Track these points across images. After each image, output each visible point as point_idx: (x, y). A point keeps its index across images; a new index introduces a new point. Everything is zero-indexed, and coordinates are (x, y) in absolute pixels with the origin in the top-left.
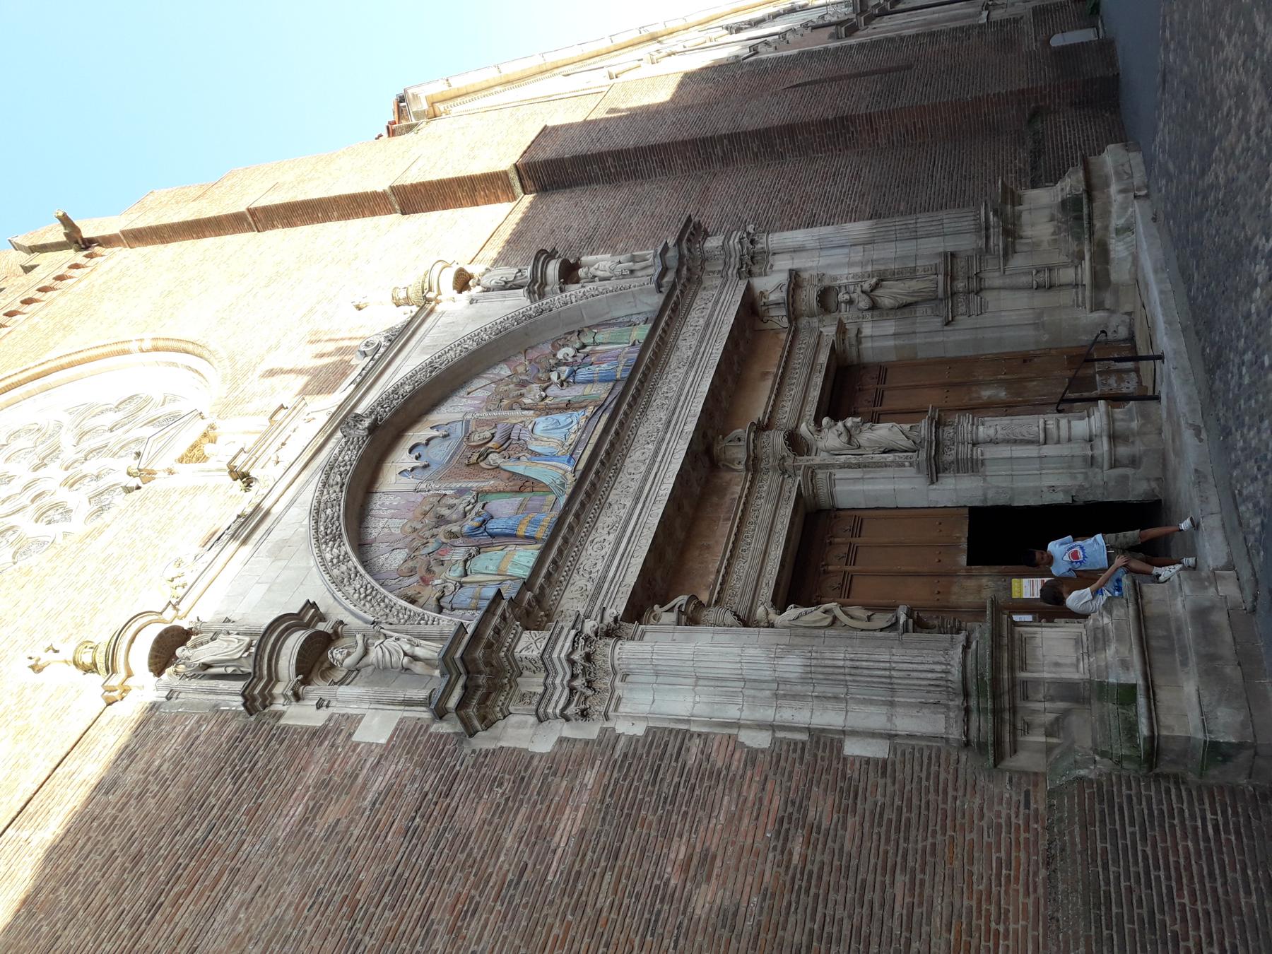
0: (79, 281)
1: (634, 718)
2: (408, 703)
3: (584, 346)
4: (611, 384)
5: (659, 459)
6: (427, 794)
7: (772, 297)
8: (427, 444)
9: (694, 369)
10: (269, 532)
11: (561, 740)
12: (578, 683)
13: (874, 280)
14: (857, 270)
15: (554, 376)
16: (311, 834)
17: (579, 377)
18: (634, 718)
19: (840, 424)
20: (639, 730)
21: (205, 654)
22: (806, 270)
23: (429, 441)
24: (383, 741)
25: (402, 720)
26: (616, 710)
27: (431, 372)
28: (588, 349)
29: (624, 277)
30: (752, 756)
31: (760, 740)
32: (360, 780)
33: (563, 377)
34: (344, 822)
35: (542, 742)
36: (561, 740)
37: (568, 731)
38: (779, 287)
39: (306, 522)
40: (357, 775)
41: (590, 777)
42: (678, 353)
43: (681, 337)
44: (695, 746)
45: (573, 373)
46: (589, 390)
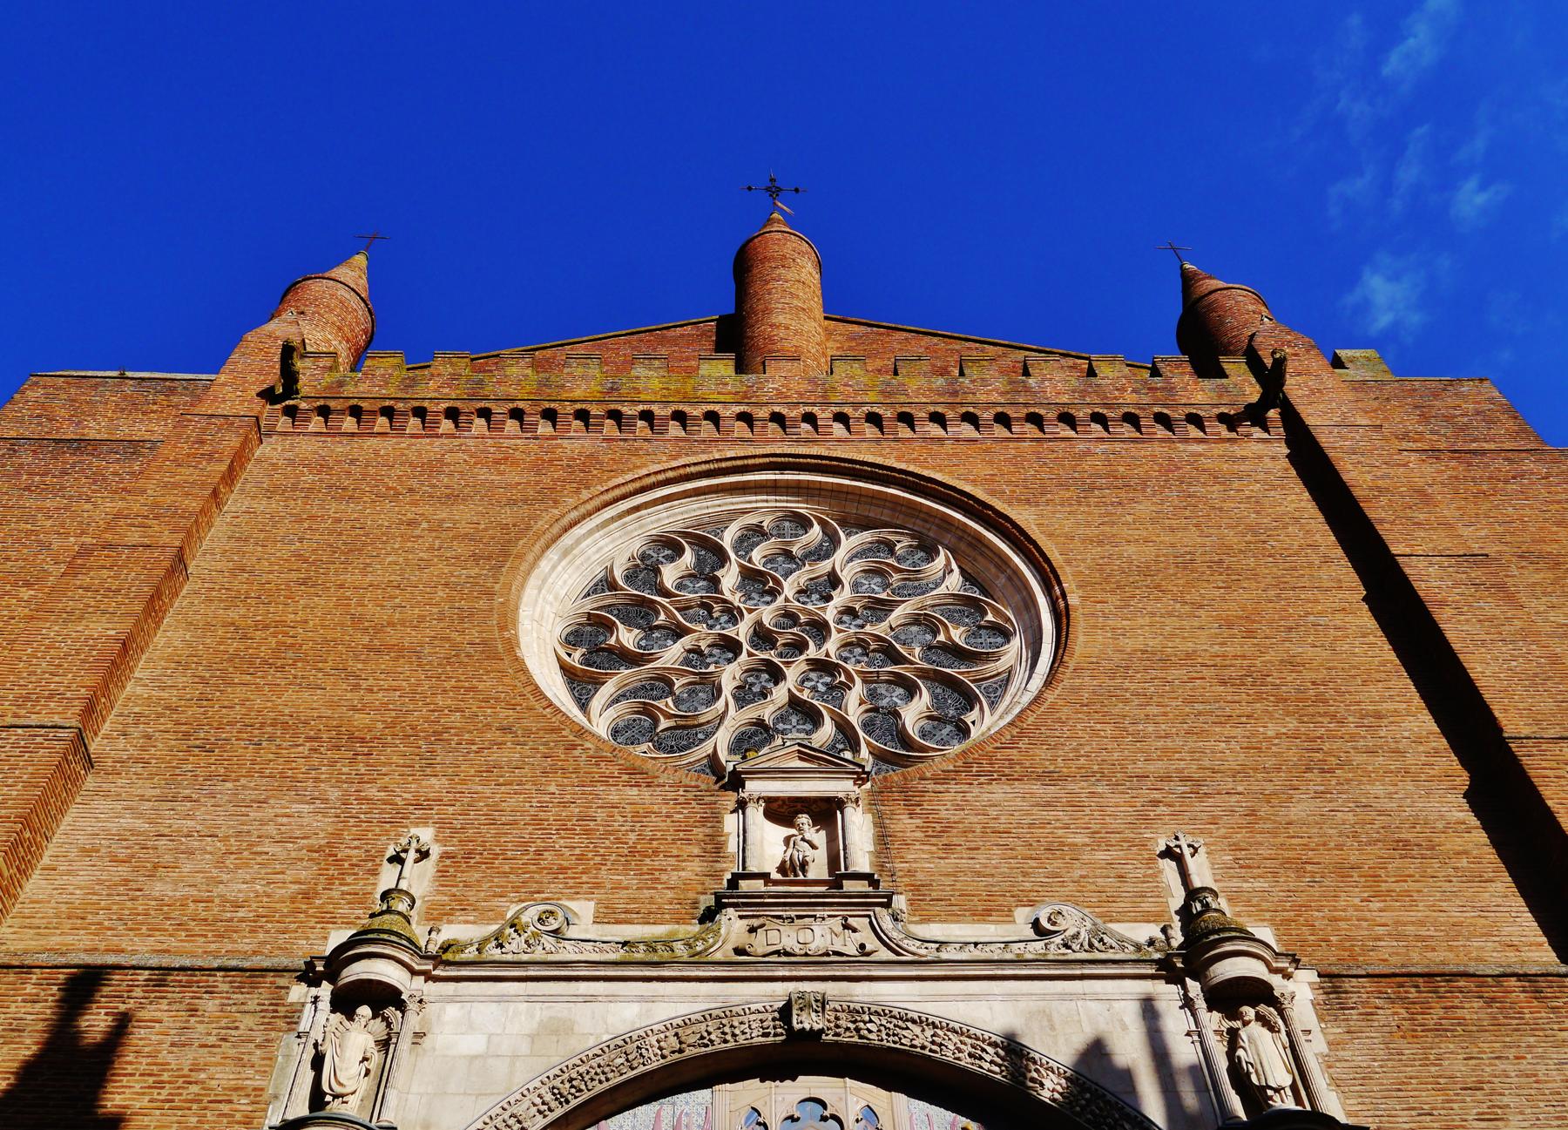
8: (824, 1119)
10: (590, 999)
23: (835, 1118)
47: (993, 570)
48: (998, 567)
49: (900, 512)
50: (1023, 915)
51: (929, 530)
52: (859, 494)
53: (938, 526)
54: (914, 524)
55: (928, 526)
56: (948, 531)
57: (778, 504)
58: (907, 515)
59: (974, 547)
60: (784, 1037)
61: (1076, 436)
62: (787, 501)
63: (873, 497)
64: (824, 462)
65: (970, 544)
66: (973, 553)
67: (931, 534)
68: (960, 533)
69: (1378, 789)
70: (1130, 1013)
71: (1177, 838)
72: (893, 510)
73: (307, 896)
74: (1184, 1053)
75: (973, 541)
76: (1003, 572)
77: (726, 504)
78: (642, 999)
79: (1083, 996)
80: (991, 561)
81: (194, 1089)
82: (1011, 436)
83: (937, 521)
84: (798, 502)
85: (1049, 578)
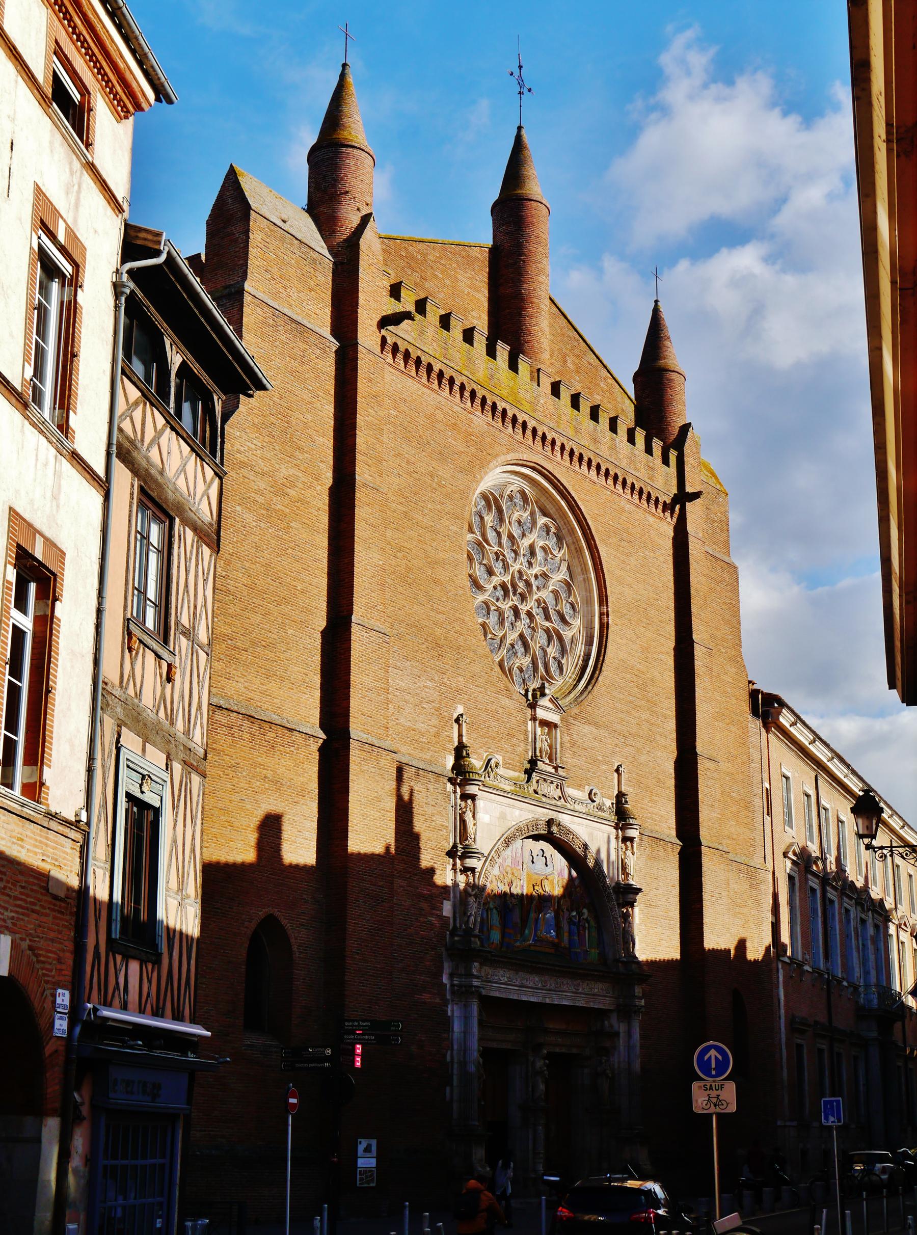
0: (654, 515)
1: (453, 1011)
2: (455, 920)
3: (588, 923)
4: (567, 946)
5: (536, 991)
6: (431, 940)
7: (606, 1022)
9: (573, 995)
10: (509, 806)
11: (446, 985)
12: (464, 989)
13: (610, 1075)
14: (616, 1066)
15: (574, 913)
16: (420, 901)
17: (573, 927)
18: (453, 1011)
19: (545, 1068)
20: (449, 1013)
21: (468, 817)
22: (619, 1040)
24: (444, 914)
25: (449, 917)
26: (456, 1004)
27: (579, 847)
28: (587, 925)
29: (624, 937)
30: (445, 1056)
31: (448, 1058)
32: (434, 911)
33: (573, 919)
34: (423, 912)
35: (445, 980)
36: (446, 985)
37: (448, 986)
38: (611, 1026)
39: (514, 823)
40: (434, 909)
41: (438, 1000)
42: (581, 983)
43: (588, 982)
44: (445, 1035)
45: (574, 924)
46: (566, 936)
47: (580, 570)
48: (582, 570)
49: (559, 513)
50: (587, 789)
51: (564, 529)
52: (551, 496)
53: (568, 530)
54: (560, 522)
55: (565, 527)
56: (571, 536)
57: (522, 484)
58: (560, 516)
59: (577, 552)
60: (546, 832)
61: (623, 495)
62: (525, 484)
63: (554, 500)
64: (550, 475)
65: (576, 549)
66: (576, 555)
67: (563, 531)
68: (575, 541)
69: (659, 754)
70: (606, 835)
71: (621, 765)
72: (557, 510)
73: (437, 735)
74: (613, 857)
75: (578, 549)
76: (583, 574)
77: (509, 478)
78: (521, 809)
79: (599, 830)
80: (581, 565)
81: (434, 823)
82: (605, 484)
83: (569, 528)
84: (528, 486)
85: (603, 599)
